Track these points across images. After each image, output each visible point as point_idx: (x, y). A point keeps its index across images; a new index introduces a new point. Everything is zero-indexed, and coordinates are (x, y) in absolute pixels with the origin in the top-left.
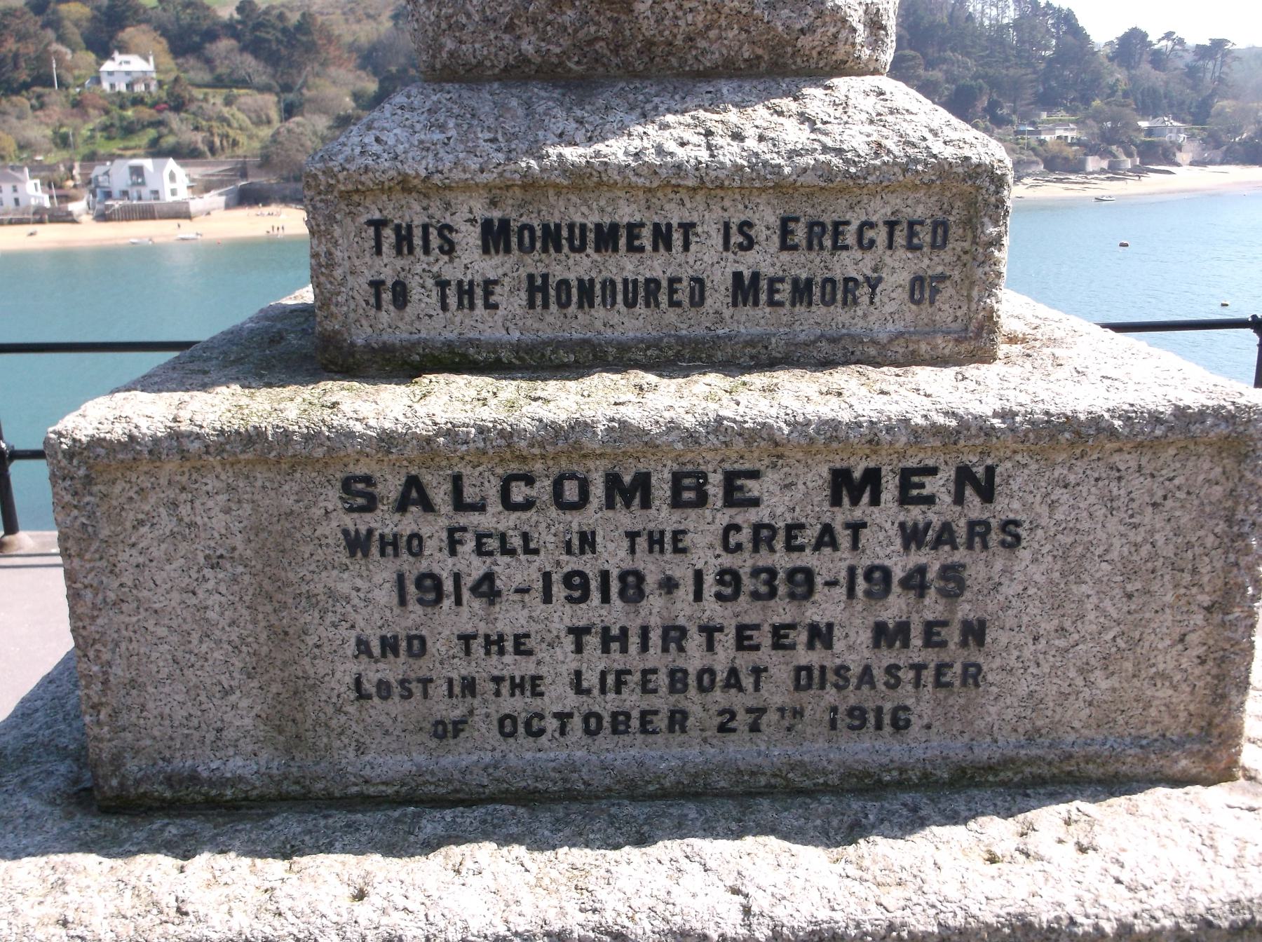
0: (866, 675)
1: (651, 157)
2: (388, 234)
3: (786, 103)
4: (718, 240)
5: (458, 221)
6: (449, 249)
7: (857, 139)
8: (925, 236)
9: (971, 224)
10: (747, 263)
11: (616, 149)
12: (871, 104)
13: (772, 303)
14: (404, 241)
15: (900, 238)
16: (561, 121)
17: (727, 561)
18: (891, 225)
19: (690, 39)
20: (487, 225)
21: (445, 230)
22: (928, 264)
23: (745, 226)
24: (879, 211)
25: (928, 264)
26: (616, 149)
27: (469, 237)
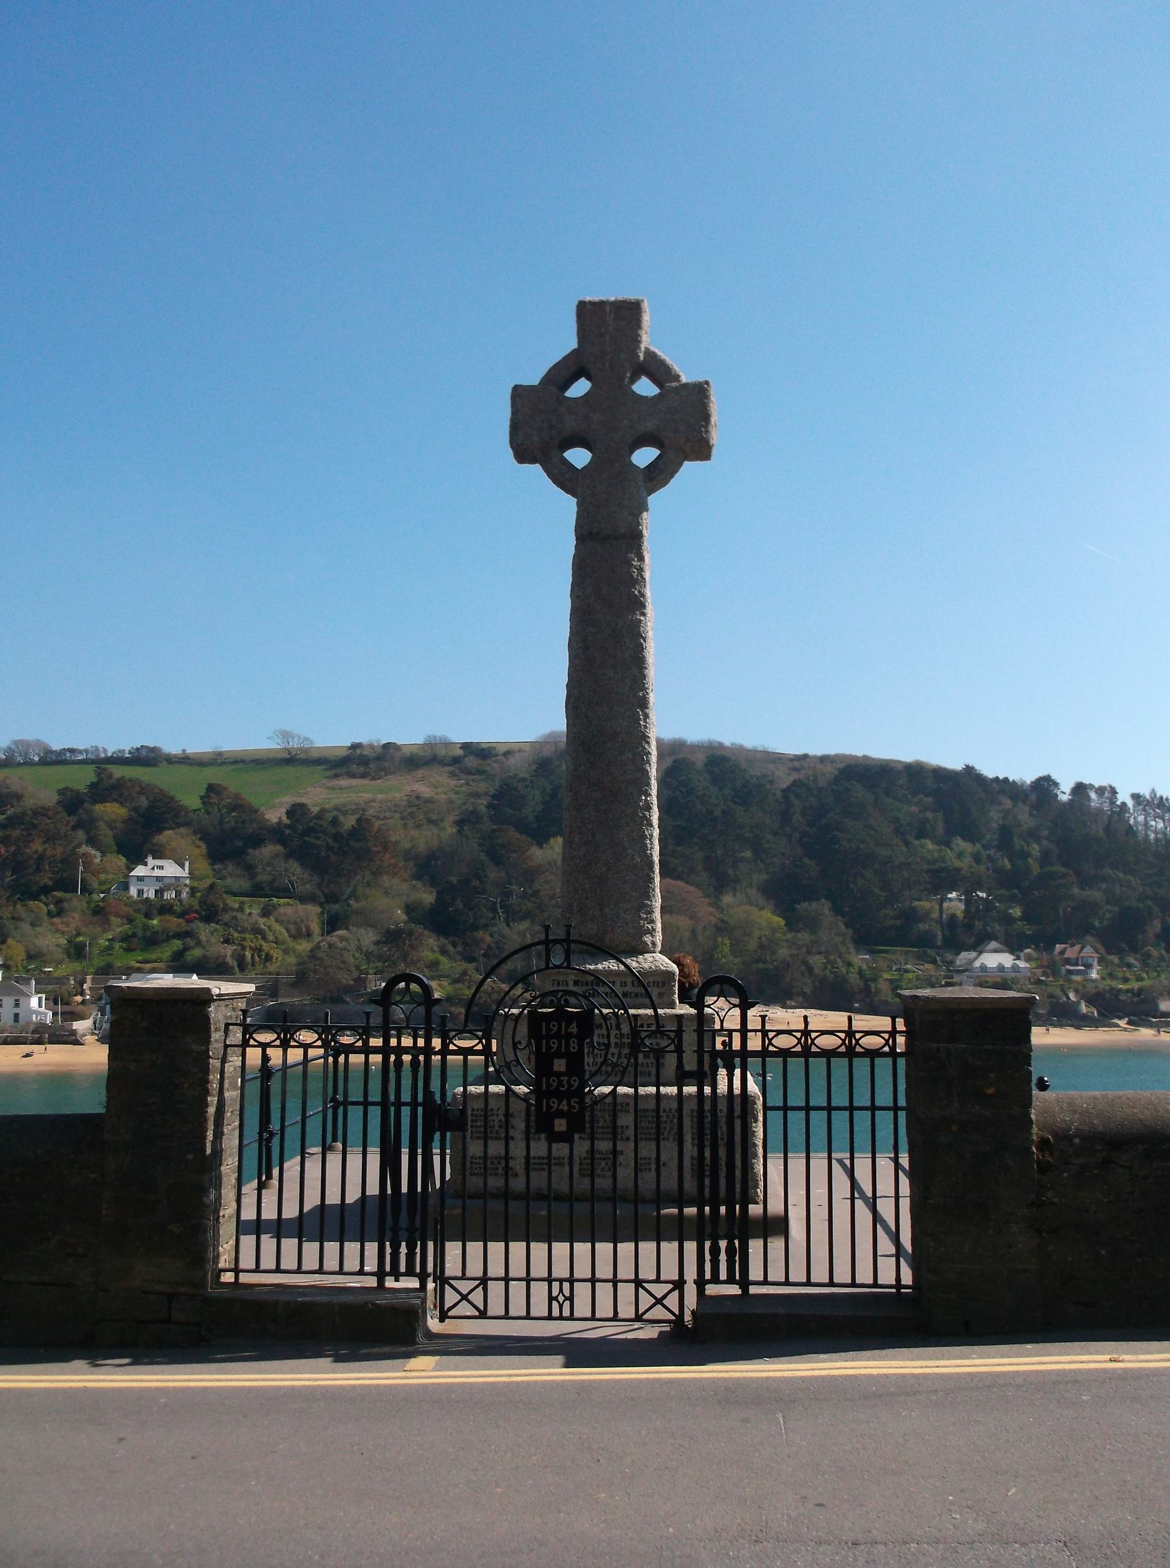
0: (643, 1064)
1: (607, 968)
2: (556, 982)
3: (635, 959)
4: (619, 984)
5: (569, 980)
6: (567, 985)
7: (646, 966)
8: (660, 985)
9: (669, 982)
10: (626, 989)
11: (600, 966)
12: (651, 959)
13: (630, 997)
14: (558, 984)
15: (656, 985)
16: (590, 961)
17: (616, 1040)
18: (654, 983)
19: (616, 946)
20: (575, 981)
21: (566, 982)
22: (662, 990)
23: (625, 982)
24: (651, 980)
25: (662, 990)
26: (600, 966)
27: (571, 983)
